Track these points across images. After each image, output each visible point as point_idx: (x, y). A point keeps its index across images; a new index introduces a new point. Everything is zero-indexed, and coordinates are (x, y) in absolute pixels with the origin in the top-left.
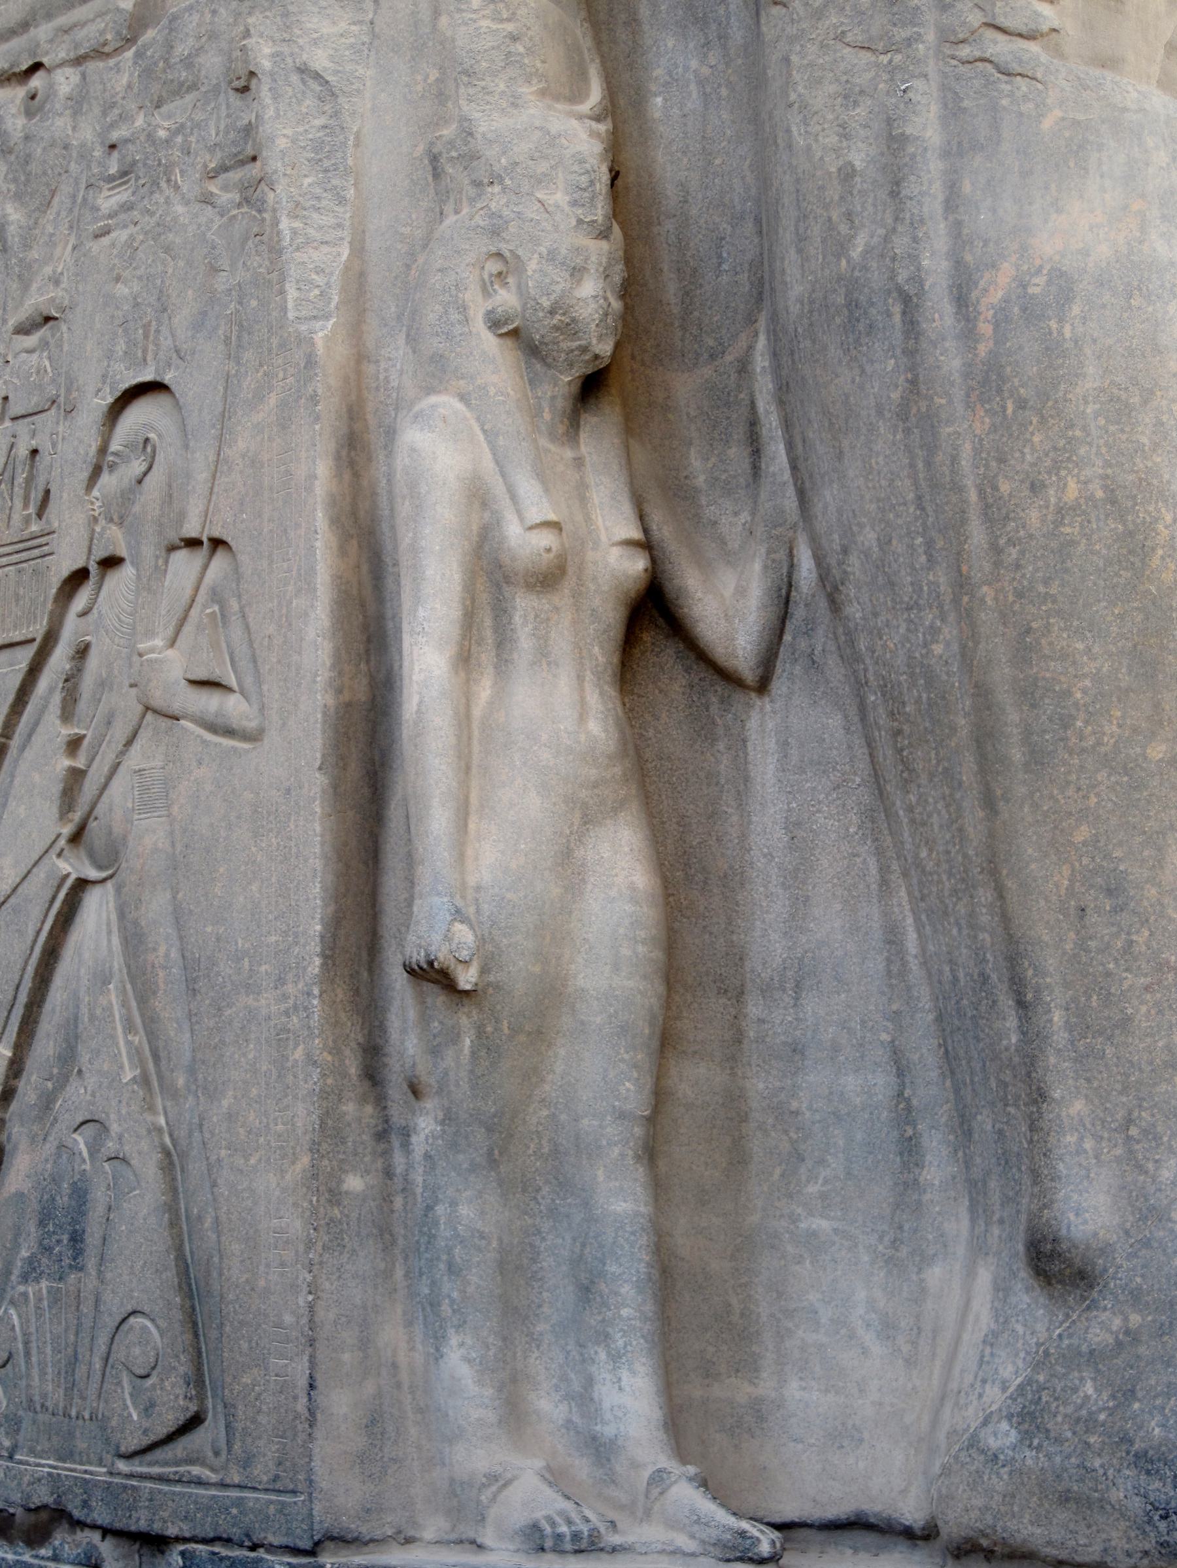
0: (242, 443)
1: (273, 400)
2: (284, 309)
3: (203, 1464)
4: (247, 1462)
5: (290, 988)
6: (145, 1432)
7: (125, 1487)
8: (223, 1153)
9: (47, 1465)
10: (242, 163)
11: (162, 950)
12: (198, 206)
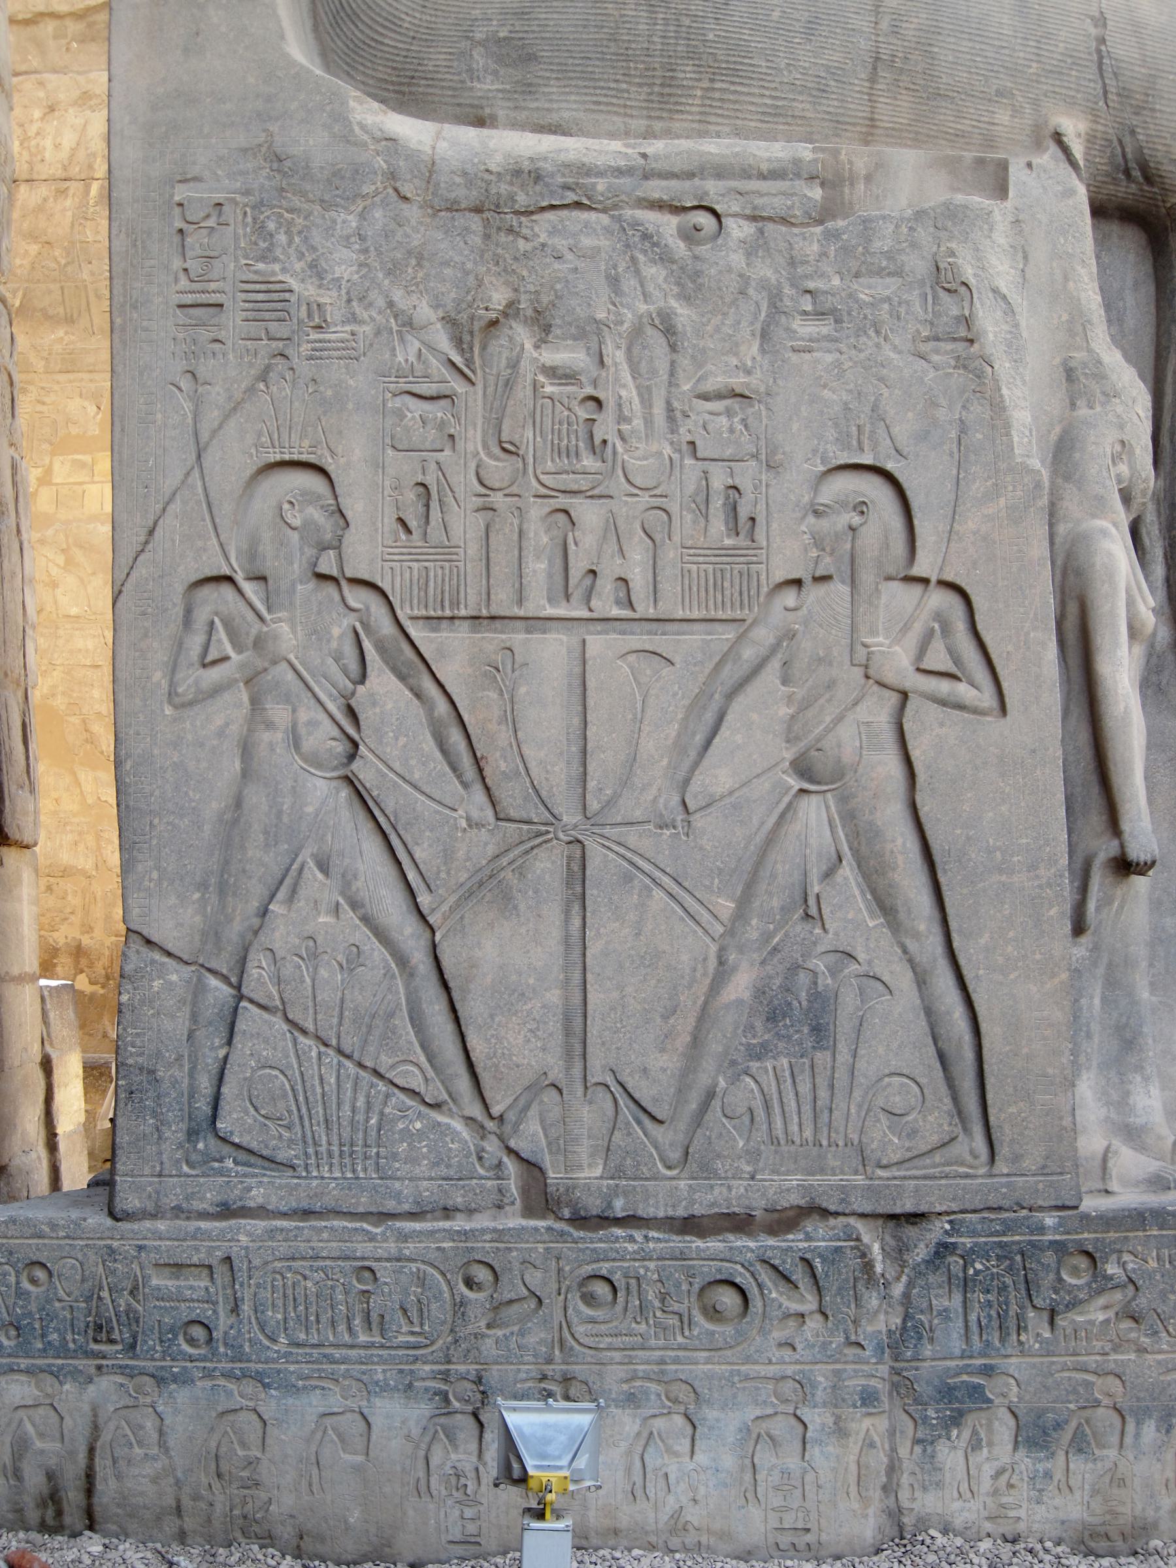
0: (971, 523)
1: (1002, 501)
3: (962, 1164)
4: (1017, 1158)
5: (1042, 872)
6: (909, 1149)
7: (888, 1186)
8: (981, 972)
9: (794, 1180)
10: (955, 340)
11: (899, 841)
12: (911, 358)
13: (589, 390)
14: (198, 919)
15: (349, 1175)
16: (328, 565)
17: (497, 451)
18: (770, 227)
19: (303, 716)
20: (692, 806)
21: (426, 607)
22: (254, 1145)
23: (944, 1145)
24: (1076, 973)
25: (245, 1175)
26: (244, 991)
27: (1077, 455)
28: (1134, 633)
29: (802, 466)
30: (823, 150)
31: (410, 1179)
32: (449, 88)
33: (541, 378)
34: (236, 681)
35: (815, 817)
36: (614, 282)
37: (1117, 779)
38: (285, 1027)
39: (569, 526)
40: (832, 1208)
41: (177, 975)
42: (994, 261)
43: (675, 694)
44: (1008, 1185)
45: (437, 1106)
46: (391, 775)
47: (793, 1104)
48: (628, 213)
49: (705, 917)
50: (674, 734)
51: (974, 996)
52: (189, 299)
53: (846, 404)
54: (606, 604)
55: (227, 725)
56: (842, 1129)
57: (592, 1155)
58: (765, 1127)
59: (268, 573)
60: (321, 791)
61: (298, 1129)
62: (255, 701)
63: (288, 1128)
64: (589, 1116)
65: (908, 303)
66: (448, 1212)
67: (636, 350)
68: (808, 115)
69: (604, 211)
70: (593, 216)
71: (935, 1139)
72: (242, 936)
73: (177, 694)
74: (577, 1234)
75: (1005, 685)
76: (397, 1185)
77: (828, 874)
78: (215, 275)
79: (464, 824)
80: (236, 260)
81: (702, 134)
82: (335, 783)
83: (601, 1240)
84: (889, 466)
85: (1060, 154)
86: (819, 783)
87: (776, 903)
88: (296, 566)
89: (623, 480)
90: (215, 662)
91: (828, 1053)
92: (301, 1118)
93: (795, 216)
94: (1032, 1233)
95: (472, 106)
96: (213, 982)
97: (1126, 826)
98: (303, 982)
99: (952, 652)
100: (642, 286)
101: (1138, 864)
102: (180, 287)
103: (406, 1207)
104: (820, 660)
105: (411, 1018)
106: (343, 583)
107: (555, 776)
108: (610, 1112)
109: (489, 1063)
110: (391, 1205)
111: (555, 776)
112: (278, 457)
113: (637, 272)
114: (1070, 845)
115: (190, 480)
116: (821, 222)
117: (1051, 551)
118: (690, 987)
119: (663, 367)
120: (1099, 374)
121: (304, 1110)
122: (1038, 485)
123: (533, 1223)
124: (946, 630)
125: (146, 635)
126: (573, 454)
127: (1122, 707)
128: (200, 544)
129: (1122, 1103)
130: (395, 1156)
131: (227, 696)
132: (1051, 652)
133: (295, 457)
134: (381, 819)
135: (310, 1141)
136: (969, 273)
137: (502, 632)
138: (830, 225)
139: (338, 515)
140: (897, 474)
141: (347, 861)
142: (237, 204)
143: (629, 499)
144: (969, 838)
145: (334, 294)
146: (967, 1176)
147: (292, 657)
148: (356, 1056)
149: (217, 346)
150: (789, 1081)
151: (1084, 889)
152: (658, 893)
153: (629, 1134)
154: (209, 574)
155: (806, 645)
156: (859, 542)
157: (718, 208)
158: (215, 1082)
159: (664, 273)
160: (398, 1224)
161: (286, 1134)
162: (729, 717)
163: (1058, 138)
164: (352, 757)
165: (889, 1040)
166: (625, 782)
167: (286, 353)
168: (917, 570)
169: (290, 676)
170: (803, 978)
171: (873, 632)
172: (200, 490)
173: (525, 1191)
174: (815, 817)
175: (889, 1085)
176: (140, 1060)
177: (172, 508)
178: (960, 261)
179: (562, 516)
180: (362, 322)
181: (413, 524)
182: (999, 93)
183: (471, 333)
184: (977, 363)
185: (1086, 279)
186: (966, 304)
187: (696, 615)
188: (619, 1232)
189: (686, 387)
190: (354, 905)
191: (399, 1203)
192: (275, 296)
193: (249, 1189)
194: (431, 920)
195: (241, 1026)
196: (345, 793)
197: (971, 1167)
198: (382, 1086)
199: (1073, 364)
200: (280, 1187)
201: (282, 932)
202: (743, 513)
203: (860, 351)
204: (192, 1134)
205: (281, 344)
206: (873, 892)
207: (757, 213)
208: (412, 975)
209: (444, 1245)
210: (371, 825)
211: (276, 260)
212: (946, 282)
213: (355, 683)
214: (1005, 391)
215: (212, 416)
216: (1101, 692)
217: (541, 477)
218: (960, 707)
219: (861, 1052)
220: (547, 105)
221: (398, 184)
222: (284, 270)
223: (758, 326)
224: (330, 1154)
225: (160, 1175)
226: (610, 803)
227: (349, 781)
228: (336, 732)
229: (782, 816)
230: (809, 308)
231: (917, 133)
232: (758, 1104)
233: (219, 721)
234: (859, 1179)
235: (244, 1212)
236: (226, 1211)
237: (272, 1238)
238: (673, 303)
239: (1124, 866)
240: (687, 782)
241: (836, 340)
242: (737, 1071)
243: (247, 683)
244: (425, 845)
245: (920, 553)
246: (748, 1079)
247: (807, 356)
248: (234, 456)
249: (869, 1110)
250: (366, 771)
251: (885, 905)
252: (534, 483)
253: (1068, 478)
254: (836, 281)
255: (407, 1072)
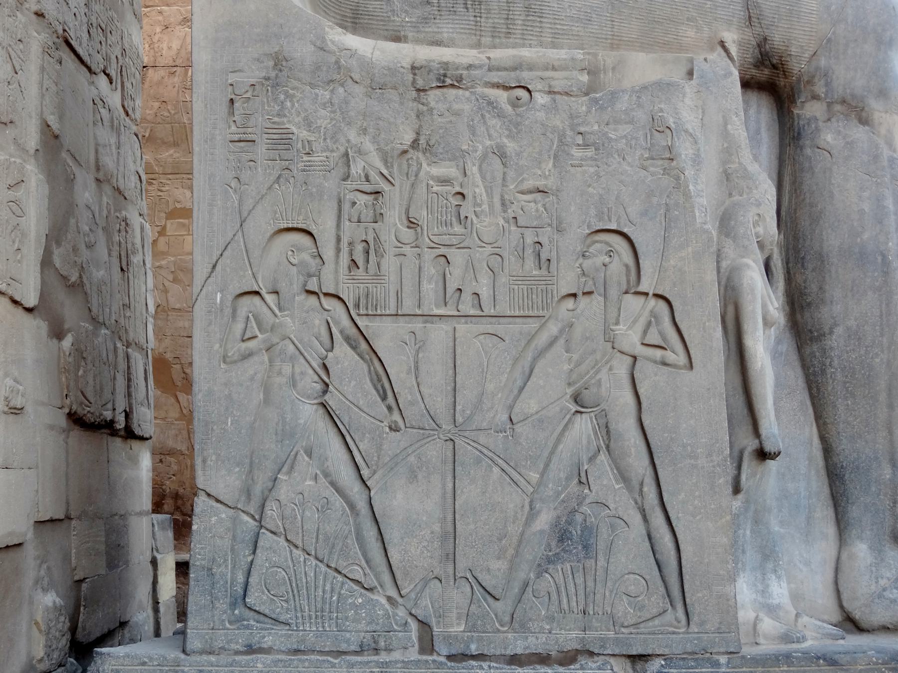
1: (690, 249)
2: (694, 217)
3: (671, 626)
4: (702, 623)
6: (640, 617)
7: (627, 639)
8: (680, 515)
9: (574, 634)
10: (663, 159)
11: (633, 440)
12: (638, 169)
13: (458, 189)
14: (237, 482)
15: (321, 629)
16: (313, 285)
17: (406, 222)
18: (558, 97)
19: (298, 370)
20: (515, 421)
21: (367, 309)
22: (267, 612)
23: (660, 614)
24: (736, 517)
25: (262, 629)
26: (263, 523)
27: (733, 223)
28: (767, 323)
29: (576, 231)
30: (589, 54)
31: (356, 632)
32: (382, 21)
33: (431, 182)
34: (261, 349)
35: (583, 426)
36: (473, 130)
37: (758, 406)
38: (286, 544)
39: (447, 264)
40: (596, 651)
41: (225, 514)
42: (685, 114)
43: (506, 358)
44: (698, 639)
45: (370, 590)
46: (347, 402)
47: (573, 590)
48: (479, 90)
49: (522, 482)
50: (504, 380)
51: (676, 529)
52: (236, 137)
53: (601, 195)
54: (467, 307)
55: (256, 374)
56: (601, 605)
57: (459, 618)
58: (557, 603)
59: (278, 290)
60: (309, 412)
61: (292, 602)
62: (271, 361)
63: (287, 601)
64: (458, 596)
65: (636, 139)
66: (376, 651)
67: (484, 166)
68: (581, 34)
69: (467, 89)
70: (461, 92)
71: (655, 611)
72: (263, 492)
73: (229, 357)
74: (449, 664)
75: (692, 352)
76: (348, 635)
77: (591, 459)
78: (250, 124)
79: (387, 430)
80: (263, 116)
81: (523, 46)
82: (315, 407)
83: (463, 668)
84: (625, 230)
85: (723, 54)
86: (587, 408)
87: (562, 475)
88: (295, 286)
89: (477, 239)
90: (249, 339)
91: (593, 561)
92: (294, 596)
93: (572, 91)
94: (712, 667)
95: (393, 30)
96: (246, 518)
97: (763, 431)
98: (296, 518)
99: (662, 335)
100: (487, 130)
101: (770, 454)
102: (231, 131)
103: (353, 648)
104: (587, 339)
105: (357, 539)
106: (321, 296)
107: (440, 404)
108: (470, 594)
109: (401, 565)
110: (344, 647)
111: (440, 404)
112: (286, 226)
113: (485, 123)
114: (731, 442)
115: (236, 238)
116: (586, 94)
117: (718, 277)
118: (514, 522)
119: (499, 176)
120: (747, 175)
121: (295, 592)
122: (710, 239)
123: (425, 657)
124: (658, 323)
125: (210, 324)
126: (448, 224)
127: (760, 364)
128: (242, 273)
129: (765, 592)
130: (347, 618)
131: (256, 358)
132: (719, 333)
133: (295, 226)
134: (341, 427)
135: (298, 609)
136: (671, 122)
137: (409, 323)
138: (592, 95)
139: (318, 258)
140: (629, 234)
141: (322, 450)
142: (263, 85)
143: (480, 249)
144: (672, 439)
145: (317, 135)
146: (674, 633)
147: (292, 336)
148: (325, 561)
149: (252, 163)
150: (571, 576)
151: (739, 467)
152: (496, 470)
153: (480, 606)
154: (247, 290)
155: (578, 331)
156: (608, 273)
157: (529, 87)
158: (246, 575)
159: (500, 124)
160: (348, 658)
161: (285, 605)
162: (536, 370)
163: (722, 44)
164: (325, 392)
165: (627, 553)
166: (478, 405)
167: (290, 167)
168: (641, 288)
169: (291, 347)
170: (579, 518)
171: (617, 323)
172: (242, 244)
173: (420, 639)
174: (583, 426)
175: (628, 579)
176: (203, 562)
177: (226, 254)
178: (665, 115)
179: (443, 258)
180: (332, 151)
181: (360, 262)
182: (688, 19)
183: (392, 157)
184: (675, 172)
185: (738, 123)
186: (669, 139)
187: (517, 314)
188: (474, 663)
189: (512, 187)
190: (326, 475)
191: (349, 645)
192: (284, 136)
193: (264, 637)
194: (368, 483)
195: (261, 543)
196: (321, 411)
197: (676, 627)
198: (340, 578)
199: (730, 171)
200: (282, 636)
201: (284, 492)
202: (544, 257)
203: (609, 166)
204: (233, 605)
205: (287, 162)
206: (618, 469)
207: (552, 90)
208: (358, 514)
209: (374, 670)
210: (335, 430)
211: (285, 116)
212: (658, 126)
213: (327, 351)
214: (691, 187)
215: (249, 203)
216: (747, 355)
217: (431, 237)
218: (665, 364)
219: (611, 560)
220: (436, 30)
221: (352, 75)
222: (289, 122)
223: (552, 153)
224: (310, 617)
225: (213, 629)
226: (469, 418)
227: (323, 405)
228: (316, 378)
229: (566, 425)
230: (581, 142)
231: (642, 43)
232: (553, 589)
233: (252, 372)
234: (611, 634)
235: (261, 651)
236: (250, 650)
237: (275, 666)
238: (505, 140)
239: (763, 455)
240: (511, 407)
241: (596, 160)
242: (541, 571)
243: (267, 351)
244: (366, 441)
245: (643, 279)
246: (547, 575)
247: (579, 169)
248: (262, 223)
249: (616, 594)
250: (332, 400)
251: (623, 476)
252: (427, 239)
253: (727, 235)
254: (596, 127)
255: (354, 570)
